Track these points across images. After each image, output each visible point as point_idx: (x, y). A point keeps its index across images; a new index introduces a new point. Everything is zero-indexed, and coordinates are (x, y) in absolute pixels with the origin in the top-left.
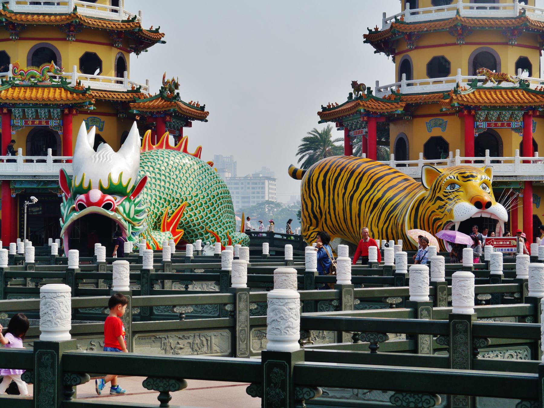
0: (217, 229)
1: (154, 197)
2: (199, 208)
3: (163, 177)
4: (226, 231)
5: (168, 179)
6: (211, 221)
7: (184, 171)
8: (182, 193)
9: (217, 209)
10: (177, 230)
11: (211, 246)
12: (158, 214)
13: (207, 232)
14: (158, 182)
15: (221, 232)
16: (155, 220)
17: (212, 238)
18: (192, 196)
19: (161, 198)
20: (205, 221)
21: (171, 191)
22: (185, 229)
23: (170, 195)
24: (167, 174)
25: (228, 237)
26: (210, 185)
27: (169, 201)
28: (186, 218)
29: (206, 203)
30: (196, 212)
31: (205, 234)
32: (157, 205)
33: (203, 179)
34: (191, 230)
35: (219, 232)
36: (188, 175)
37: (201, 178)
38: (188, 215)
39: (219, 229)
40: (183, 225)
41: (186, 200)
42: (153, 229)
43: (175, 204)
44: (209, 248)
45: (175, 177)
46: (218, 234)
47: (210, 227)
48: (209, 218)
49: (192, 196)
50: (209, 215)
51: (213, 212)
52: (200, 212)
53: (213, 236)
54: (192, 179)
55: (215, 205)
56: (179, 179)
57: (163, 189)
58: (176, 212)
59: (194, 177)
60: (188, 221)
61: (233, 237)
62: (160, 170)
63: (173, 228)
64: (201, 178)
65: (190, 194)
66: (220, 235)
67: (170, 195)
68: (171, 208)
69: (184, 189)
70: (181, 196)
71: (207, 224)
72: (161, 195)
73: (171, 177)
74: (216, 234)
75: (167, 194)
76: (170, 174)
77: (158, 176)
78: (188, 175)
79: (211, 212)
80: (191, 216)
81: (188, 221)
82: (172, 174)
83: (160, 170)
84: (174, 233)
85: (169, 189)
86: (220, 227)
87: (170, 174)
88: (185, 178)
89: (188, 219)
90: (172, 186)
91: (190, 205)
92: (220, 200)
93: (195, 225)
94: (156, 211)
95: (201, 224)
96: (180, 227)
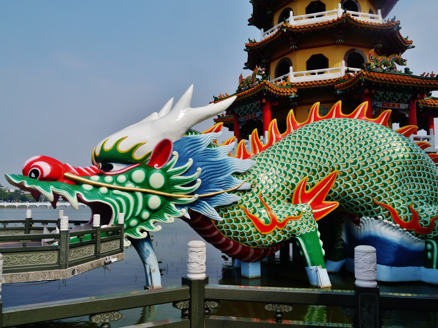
0: (391, 200)
1: (293, 167)
2: (358, 177)
3: (309, 146)
4: (409, 203)
5: (316, 147)
6: (381, 192)
7: (339, 137)
8: (333, 162)
9: (389, 177)
10: (324, 202)
11: (385, 221)
12: (297, 185)
13: (376, 205)
14: (302, 151)
15: (400, 205)
16: (291, 192)
17: (383, 211)
18: (347, 164)
19: (302, 168)
20: (369, 192)
21: (317, 160)
22: (342, 202)
23: (316, 164)
24: (315, 143)
25: (411, 210)
26: (377, 150)
27: (314, 171)
28: (341, 189)
29: (370, 170)
30: (355, 181)
31: (374, 207)
32: (296, 175)
33: (366, 143)
34: (352, 201)
35: (396, 205)
36: (344, 141)
37: (363, 143)
38: (341, 185)
39: (394, 201)
40: (339, 197)
41: (339, 168)
42: (289, 201)
43: (323, 173)
44: (382, 223)
45: (325, 144)
46: (393, 206)
47: (380, 199)
48: (377, 188)
49: (347, 164)
50: (375, 184)
51: (383, 181)
52: (362, 181)
53: (386, 210)
54: (349, 145)
55: (385, 172)
56: (330, 146)
57: (306, 158)
58: (322, 180)
59: (353, 142)
60: (344, 192)
61: (422, 211)
62: (307, 139)
63: (295, 199)
64: (363, 143)
65: (344, 161)
66: (396, 208)
67: (316, 164)
68: (318, 178)
69: (337, 156)
70: (331, 164)
71: (375, 195)
72: (303, 165)
73: (320, 145)
74: (391, 206)
75: (312, 163)
76: (319, 142)
77: (304, 145)
78: (344, 141)
79: (379, 180)
80: (348, 186)
81: (344, 192)
82: (321, 141)
83: (307, 139)
84: (314, 205)
85: (314, 157)
86: (397, 198)
87: (319, 142)
88: (340, 145)
89: (343, 190)
90: (319, 155)
91: (344, 174)
92: (394, 165)
93: (355, 197)
94: (293, 181)
95: (365, 195)
96: (336, 199)
